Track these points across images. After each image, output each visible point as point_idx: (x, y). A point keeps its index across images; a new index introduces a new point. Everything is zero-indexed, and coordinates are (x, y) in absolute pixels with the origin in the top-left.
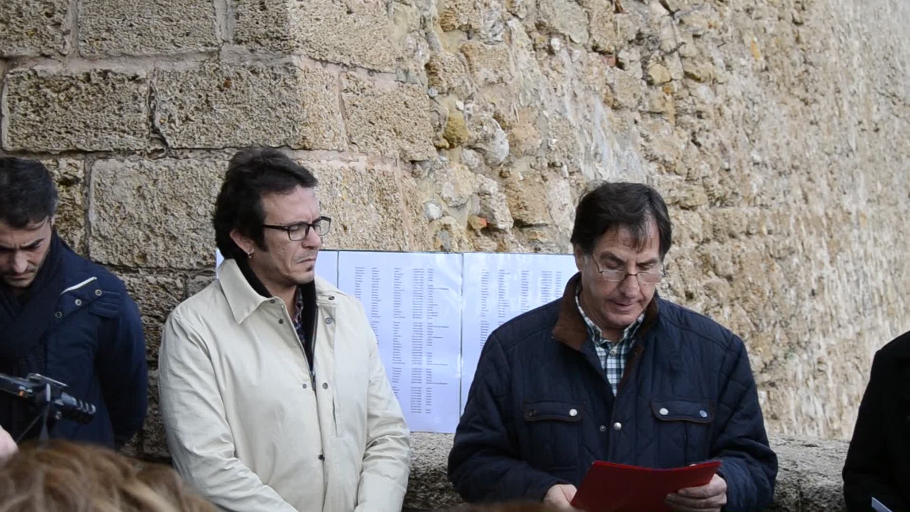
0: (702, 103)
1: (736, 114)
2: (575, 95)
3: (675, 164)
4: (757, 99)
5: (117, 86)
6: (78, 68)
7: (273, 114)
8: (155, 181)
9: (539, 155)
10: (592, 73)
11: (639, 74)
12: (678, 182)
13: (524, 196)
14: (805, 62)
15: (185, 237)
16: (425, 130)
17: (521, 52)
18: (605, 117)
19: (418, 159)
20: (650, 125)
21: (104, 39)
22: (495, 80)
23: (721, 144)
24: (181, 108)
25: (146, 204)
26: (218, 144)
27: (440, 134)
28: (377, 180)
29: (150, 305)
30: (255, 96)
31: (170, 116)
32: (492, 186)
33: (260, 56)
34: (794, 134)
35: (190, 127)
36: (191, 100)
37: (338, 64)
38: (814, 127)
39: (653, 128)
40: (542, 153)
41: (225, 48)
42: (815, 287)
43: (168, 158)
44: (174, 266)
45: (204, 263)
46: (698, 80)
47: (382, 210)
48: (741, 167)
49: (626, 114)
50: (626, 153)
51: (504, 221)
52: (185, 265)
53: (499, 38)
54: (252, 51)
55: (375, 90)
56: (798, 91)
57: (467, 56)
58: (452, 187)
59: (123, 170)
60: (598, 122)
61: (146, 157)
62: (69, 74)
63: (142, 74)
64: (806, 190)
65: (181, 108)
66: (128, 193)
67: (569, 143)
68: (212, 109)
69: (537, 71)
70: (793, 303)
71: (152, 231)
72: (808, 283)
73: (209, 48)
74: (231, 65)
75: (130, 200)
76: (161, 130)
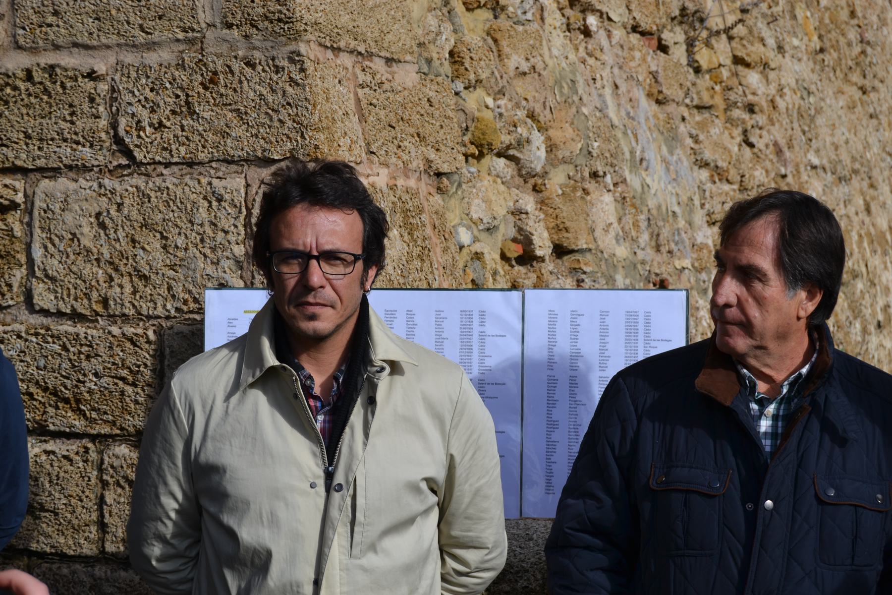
0: (754, 94)
1: (790, 106)
2: (617, 87)
3: (727, 171)
4: (813, 88)
5: (68, 85)
7: (275, 117)
8: (120, 206)
9: (578, 162)
10: (633, 58)
11: (684, 61)
12: (732, 193)
13: (565, 214)
14: (862, 42)
15: (160, 274)
16: (451, 135)
17: (555, 33)
18: (650, 114)
19: (446, 171)
20: (698, 123)
21: (50, 25)
22: (527, 70)
23: (776, 144)
24: (153, 111)
25: (106, 235)
26: (202, 156)
27: (466, 139)
28: (400, 198)
29: (114, 364)
30: (251, 94)
31: (139, 122)
32: (529, 202)
33: (257, 44)
34: (853, 131)
35: (165, 135)
36: (166, 100)
37: (351, 52)
38: (874, 122)
39: (702, 126)
40: (581, 161)
41: (210, 34)
42: (881, 317)
43: (135, 175)
44: (145, 313)
45: (185, 308)
46: (748, 65)
47: (407, 237)
48: (798, 172)
49: (671, 108)
50: (675, 158)
51: (543, 245)
52: (160, 311)
53: (529, 16)
54: (246, 37)
55: (395, 84)
56: (855, 77)
57: (495, 41)
58: (484, 205)
59: (76, 192)
60: (642, 121)
61: (107, 174)
63: (101, 68)
64: (868, 198)
65: (153, 111)
66: (84, 222)
67: (612, 147)
68: (195, 112)
69: (572, 57)
70: (859, 339)
71: (116, 270)
72: (874, 314)
73: (190, 35)
74: (219, 56)
75: (86, 229)
76: (127, 140)
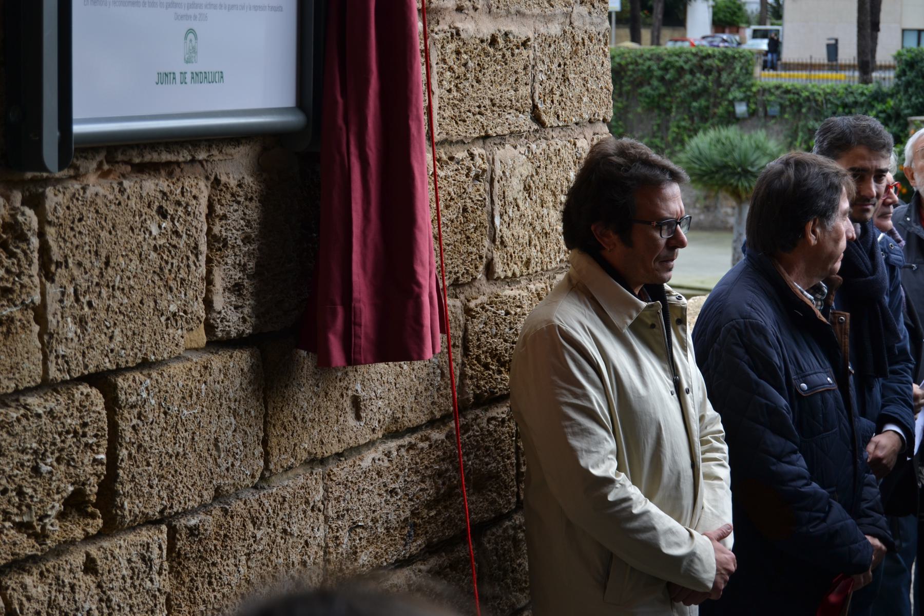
6: (487, 27)
62: (480, 36)
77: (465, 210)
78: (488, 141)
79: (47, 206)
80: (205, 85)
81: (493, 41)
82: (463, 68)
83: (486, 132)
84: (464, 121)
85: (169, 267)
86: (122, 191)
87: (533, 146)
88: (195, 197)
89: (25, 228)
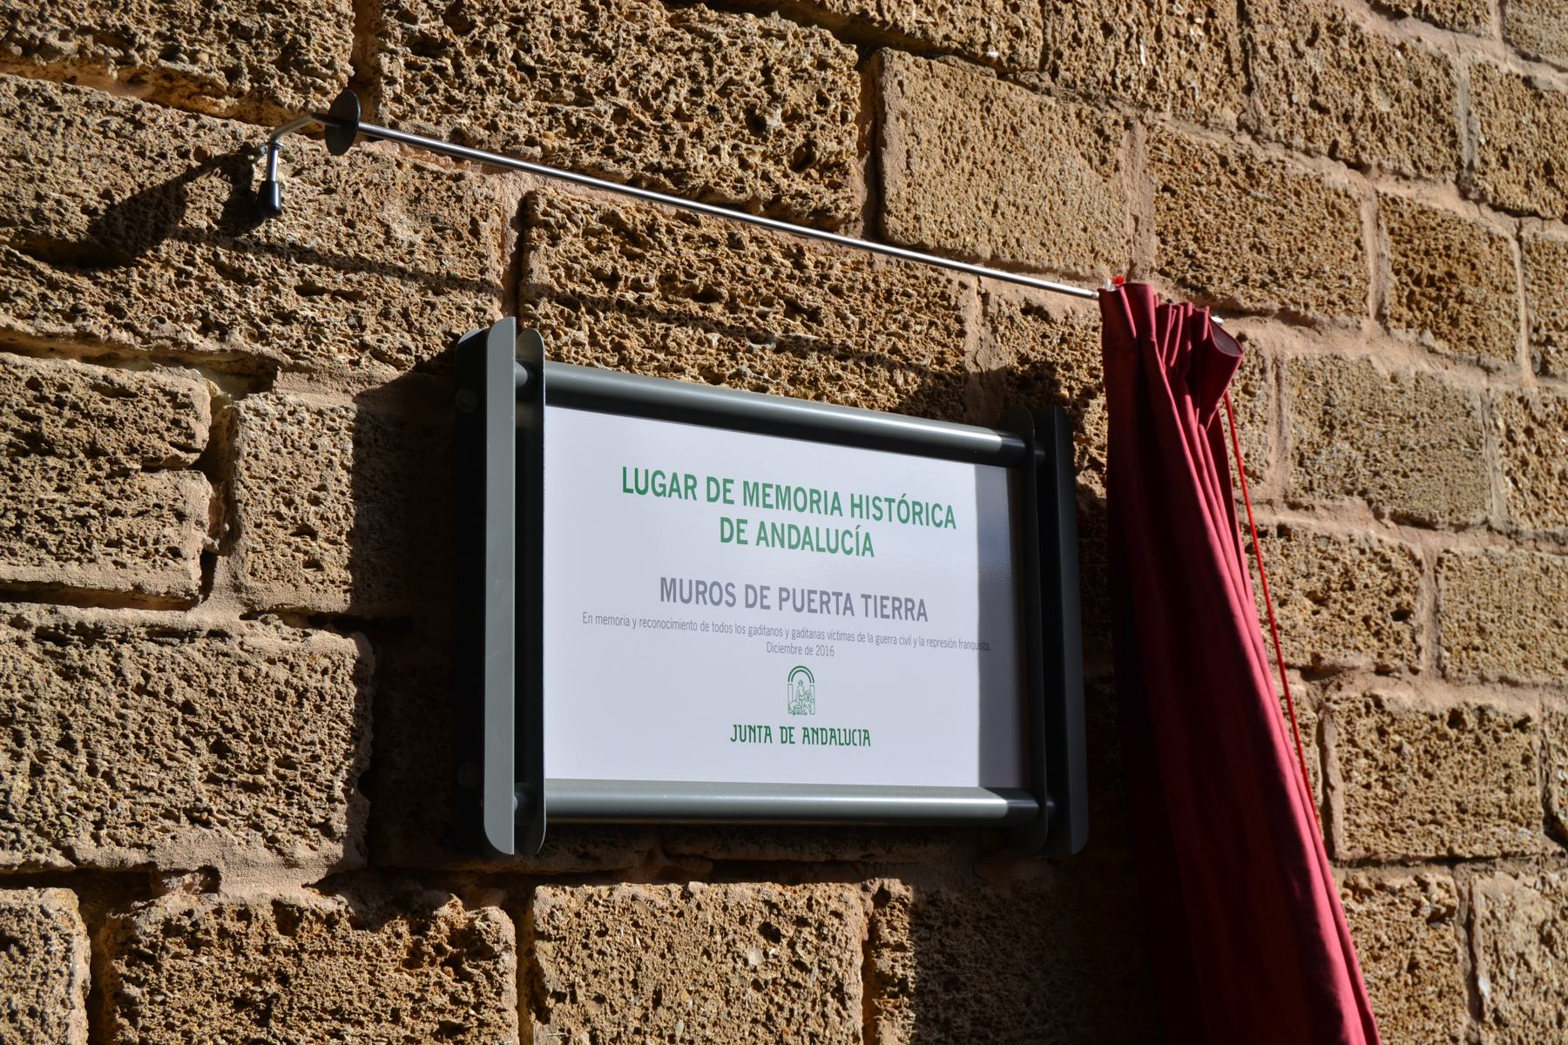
6: (1442, 698)
21: (1477, 649)
62: (1429, 709)
63: (1534, 713)
77: (1413, 966)
78: (1459, 867)
79: (536, 910)
80: (832, 749)
81: (1456, 719)
82: (1393, 755)
83: (1450, 850)
84: (1403, 832)
85: (786, 1014)
86: (687, 895)
87: (1554, 877)
88: (837, 914)
89: (489, 940)
